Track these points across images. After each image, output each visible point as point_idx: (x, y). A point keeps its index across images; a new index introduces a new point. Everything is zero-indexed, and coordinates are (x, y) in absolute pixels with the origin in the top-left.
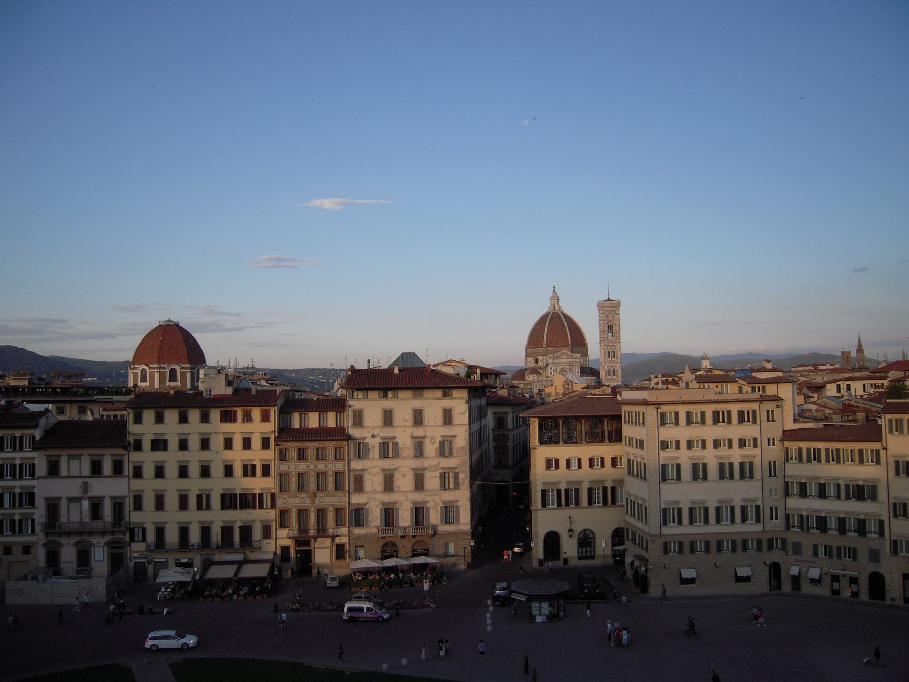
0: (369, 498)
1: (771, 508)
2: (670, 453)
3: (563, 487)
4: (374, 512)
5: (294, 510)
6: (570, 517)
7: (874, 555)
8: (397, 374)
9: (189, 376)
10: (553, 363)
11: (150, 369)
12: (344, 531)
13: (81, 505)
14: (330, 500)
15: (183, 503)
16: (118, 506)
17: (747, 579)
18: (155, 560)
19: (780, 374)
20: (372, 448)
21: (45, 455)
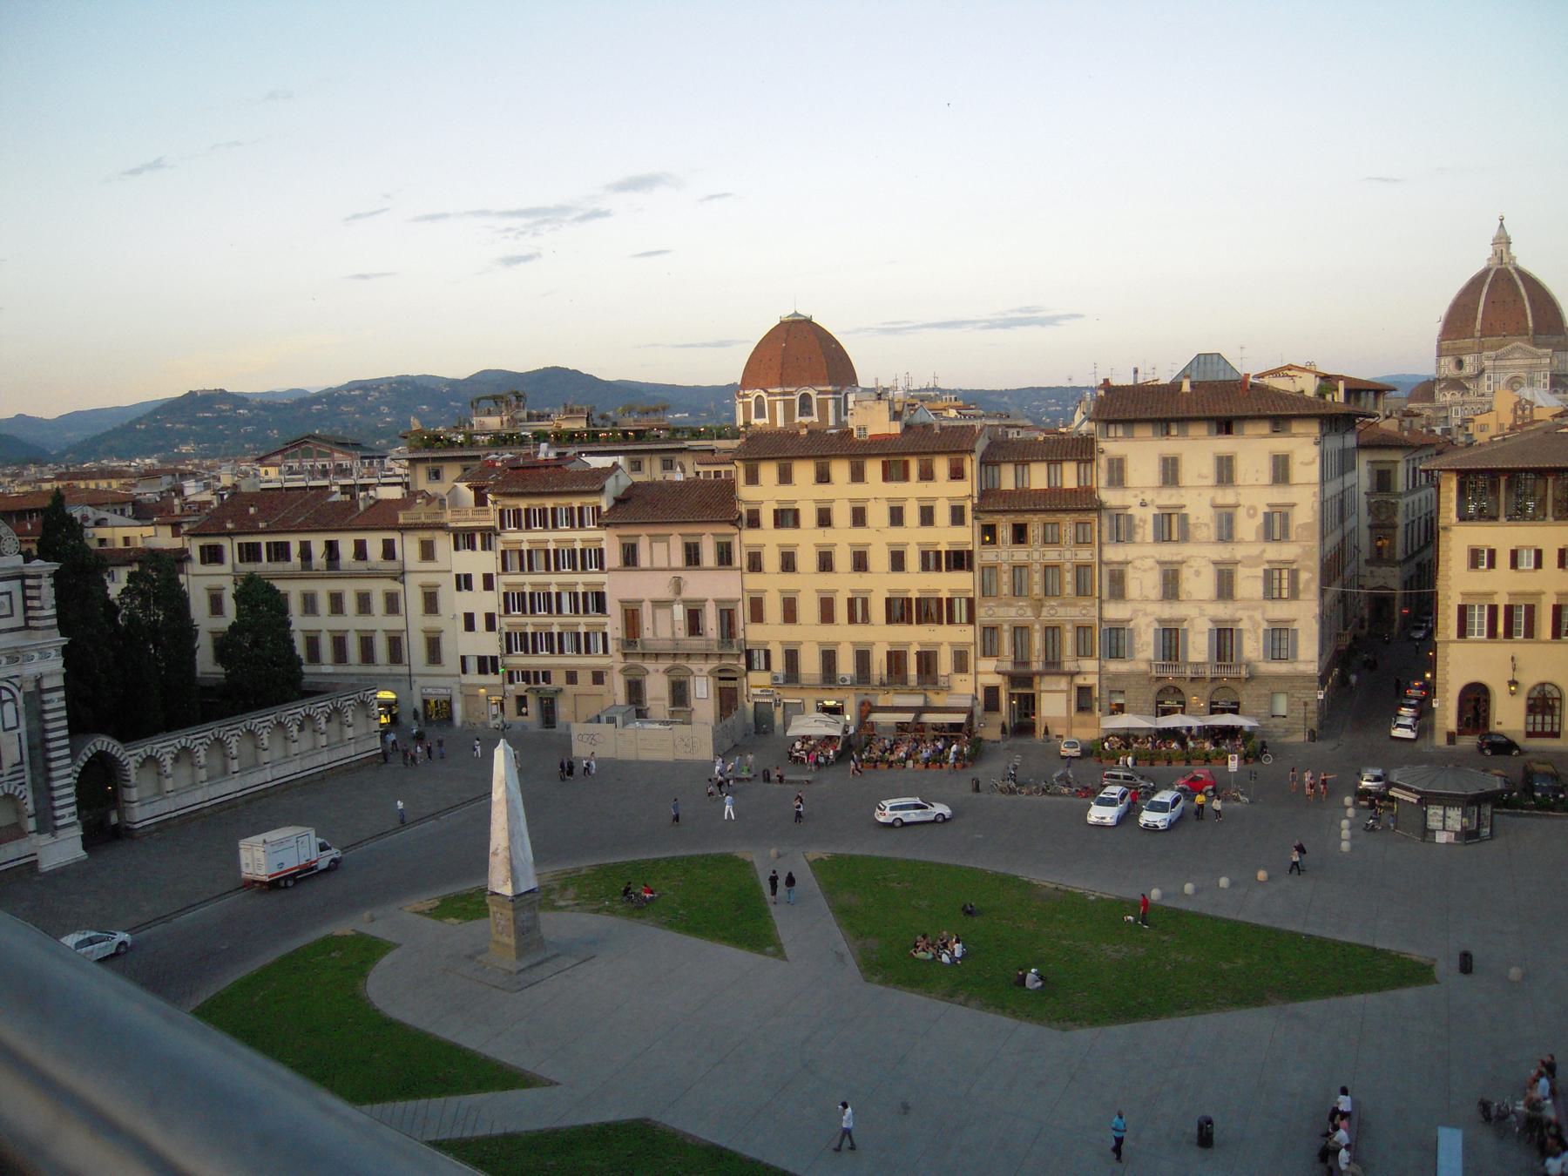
0: (1135, 611)
3: (1501, 602)
4: (1143, 635)
5: (1006, 627)
6: (1513, 659)
8: (1187, 393)
9: (831, 404)
10: (1495, 367)
11: (768, 396)
12: (1090, 665)
13: (672, 614)
14: (1068, 613)
15: (827, 613)
16: (727, 617)
18: (786, 701)
20: (1141, 524)
21: (618, 536)
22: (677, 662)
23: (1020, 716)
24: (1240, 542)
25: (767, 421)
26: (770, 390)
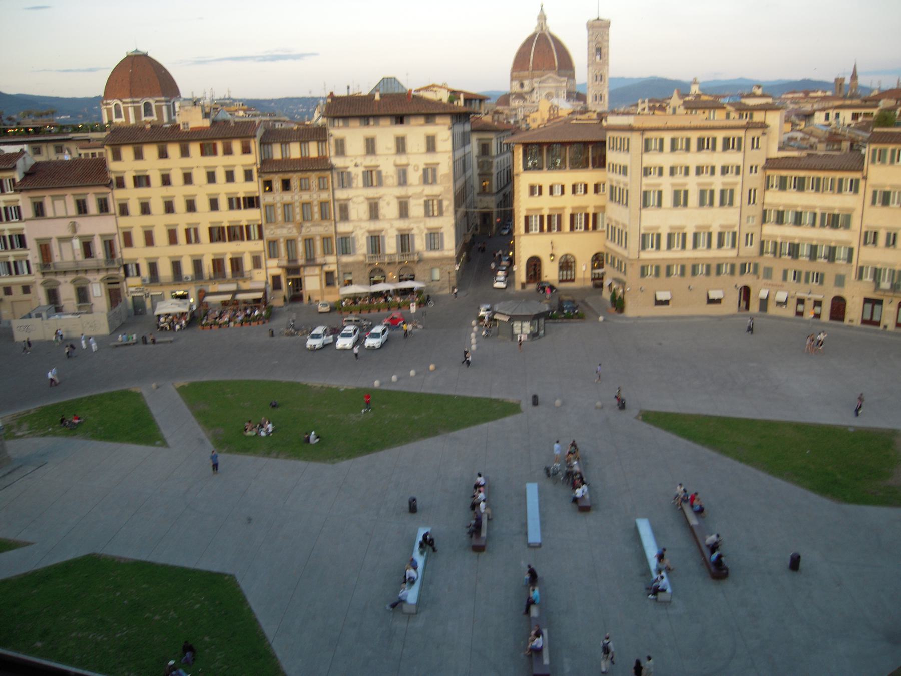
0: (355, 227)
1: (747, 235)
2: (652, 180)
5: (282, 240)
6: (552, 243)
7: (840, 281)
9: (164, 109)
10: (539, 87)
12: (331, 259)
13: (72, 245)
14: (317, 230)
15: (173, 238)
16: (109, 245)
17: (718, 301)
18: (152, 294)
19: (770, 100)
21: (31, 198)
22: (79, 275)
23: (294, 291)
24: (411, 185)
25: (123, 119)
26: (124, 100)
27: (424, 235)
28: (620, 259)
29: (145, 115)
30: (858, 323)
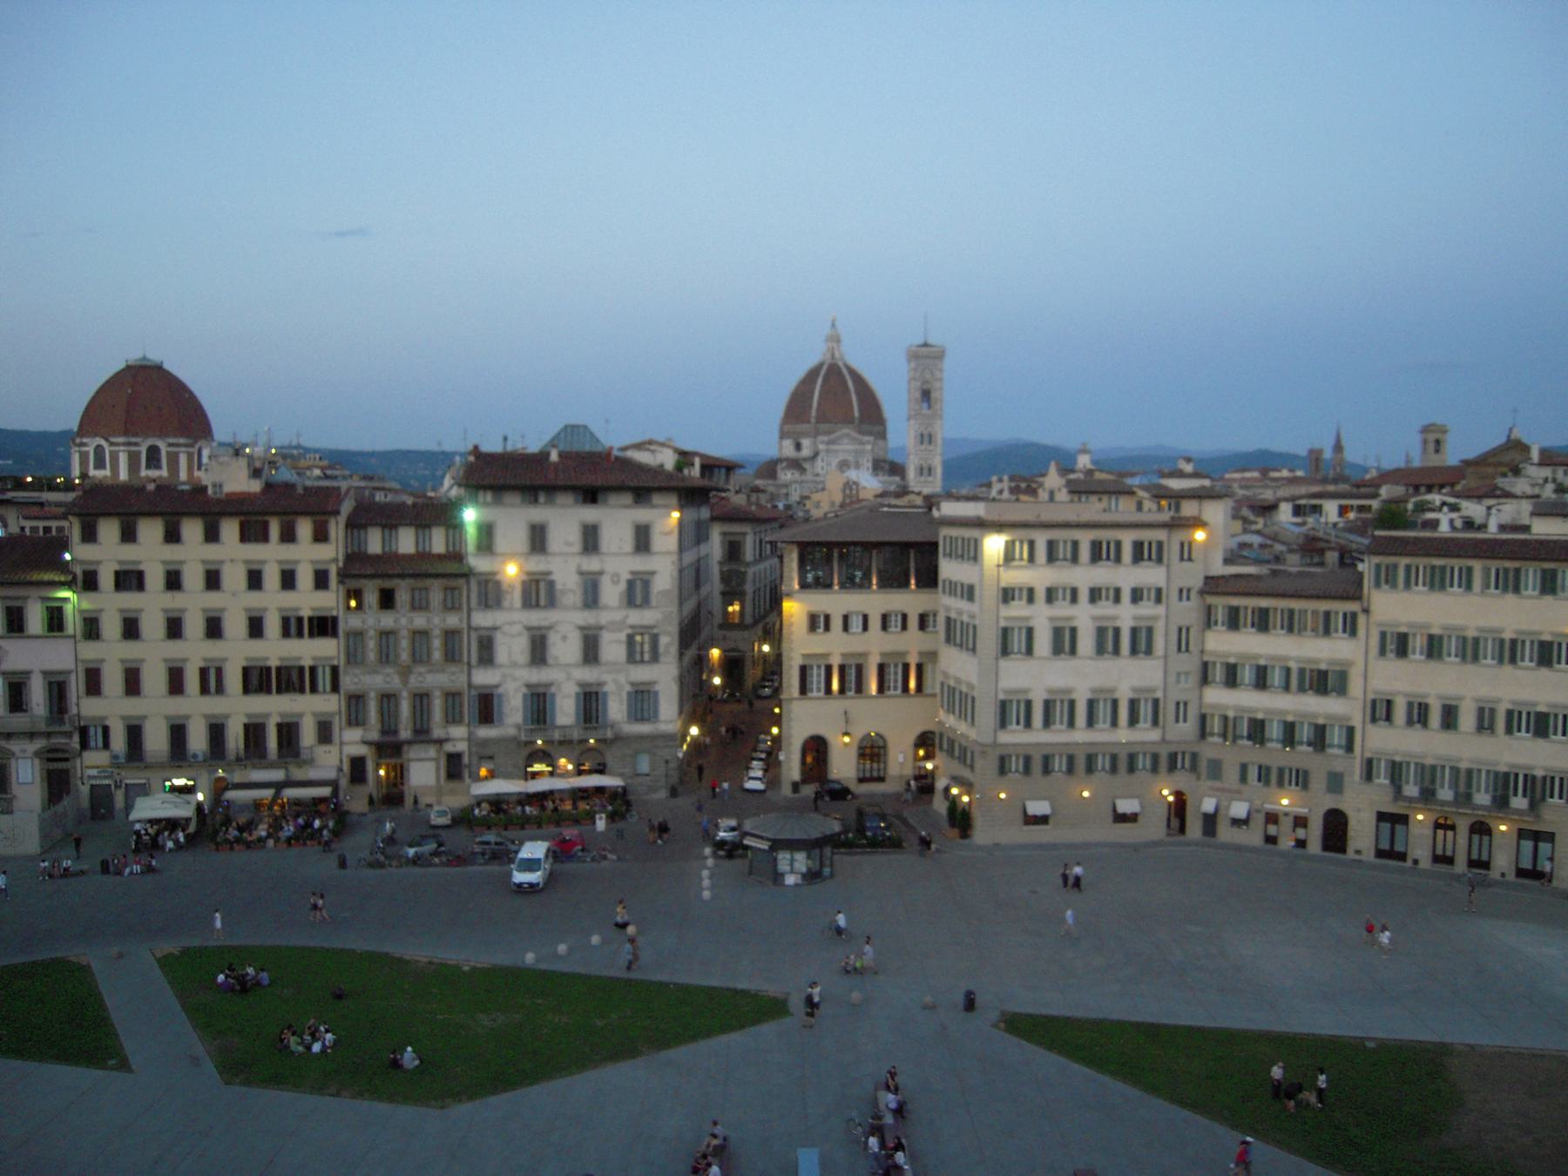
0: (504, 676)
1: (1178, 704)
2: (1018, 609)
5: (372, 695)
6: (846, 713)
7: (1336, 783)
12: (458, 732)
14: (437, 679)
15: (176, 682)
16: (57, 689)
18: (128, 781)
19: (1207, 483)
24: (606, 607)
25: (107, 472)
26: (113, 440)
27: (625, 697)
28: (964, 743)
29: (148, 467)
30: (1369, 855)
